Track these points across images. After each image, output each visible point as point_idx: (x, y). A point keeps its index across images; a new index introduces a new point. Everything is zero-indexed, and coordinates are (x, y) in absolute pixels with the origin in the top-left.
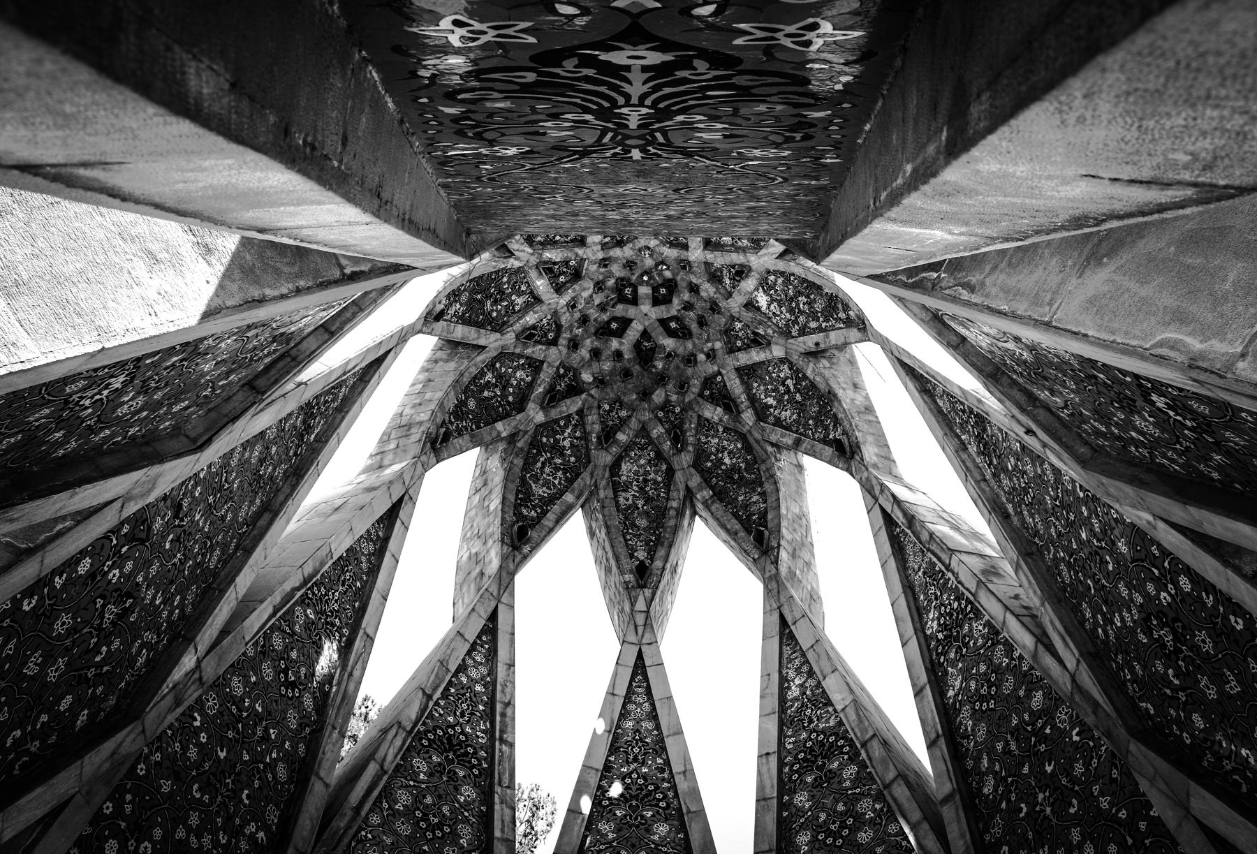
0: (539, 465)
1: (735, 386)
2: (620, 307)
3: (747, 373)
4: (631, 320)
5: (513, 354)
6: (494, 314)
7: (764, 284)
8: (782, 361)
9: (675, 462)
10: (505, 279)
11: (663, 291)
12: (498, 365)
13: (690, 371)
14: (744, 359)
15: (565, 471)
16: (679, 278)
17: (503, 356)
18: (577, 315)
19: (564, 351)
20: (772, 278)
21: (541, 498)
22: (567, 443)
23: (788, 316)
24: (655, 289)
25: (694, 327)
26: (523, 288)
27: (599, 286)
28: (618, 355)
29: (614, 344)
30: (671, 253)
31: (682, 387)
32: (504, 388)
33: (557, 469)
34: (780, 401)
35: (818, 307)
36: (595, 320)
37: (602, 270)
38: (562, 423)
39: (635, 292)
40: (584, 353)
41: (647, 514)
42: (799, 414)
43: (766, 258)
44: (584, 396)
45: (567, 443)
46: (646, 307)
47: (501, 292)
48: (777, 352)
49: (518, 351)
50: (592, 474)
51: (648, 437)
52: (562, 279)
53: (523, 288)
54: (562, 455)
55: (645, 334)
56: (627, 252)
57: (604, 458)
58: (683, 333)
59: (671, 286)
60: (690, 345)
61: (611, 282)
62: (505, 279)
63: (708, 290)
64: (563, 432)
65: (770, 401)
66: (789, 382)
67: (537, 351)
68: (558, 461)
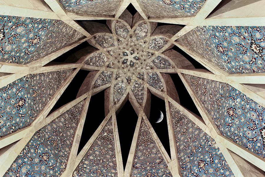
0: (160, 44)
1: (116, 43)
2: (134, 62)
3: (113, 45)
4: (133, 58)
5: (156, 66)
6: (156, 76)
7: (103, 62)
8: (105, 47)
9: (133, 33)
10: (151, 81)
11: (125, 61)
12: (160, 66)
13: (125, 47)
14: (112, 48)
15: (156, 40)
16: (121, 64)
17: (159, 68)
18: (142, 65)
19: (147, 60)
20: (102, 64)
21: (162, 40)
22: (153, 44)
23: (101, 56)
24: (126, 63)
25: (122, 54)
26: (149, 77)
27: (136, 68)
28: (138, 54)
29: (138, 55)
30: (121, 71)
31: (127, 45)
32: (161, 61)
33: (157, 42)
34: (107, 39)
35: (94, 59)
36: (139, 62)
37: (134, 72)
38: (153, 48)
39: (130, 63)
40: (144, 58)
41: (142, 26)
42: (104, 37)
43: (102, 70)
44: (147, 51)
45: (153, 44)
46: (130, 59)
47: (153, 80)
48: (105, 49)
49: (155, 67)
50: (150, 38)
51: (137, 38)
52: (142, 74)
53: (149, 77)
54: (155, 43)
55: (132, 54)
56: (129, 74)
57: (146, 39)
58: (124, 53)
59: (123, 63)
60: (123, 51)
61: (134, 68)
62: (151, 81)
63: (116, 62)
64: (153, 46)
65: (110, 39)
66: (104, 42)
67: (152, 64)
68: (156, 43)
